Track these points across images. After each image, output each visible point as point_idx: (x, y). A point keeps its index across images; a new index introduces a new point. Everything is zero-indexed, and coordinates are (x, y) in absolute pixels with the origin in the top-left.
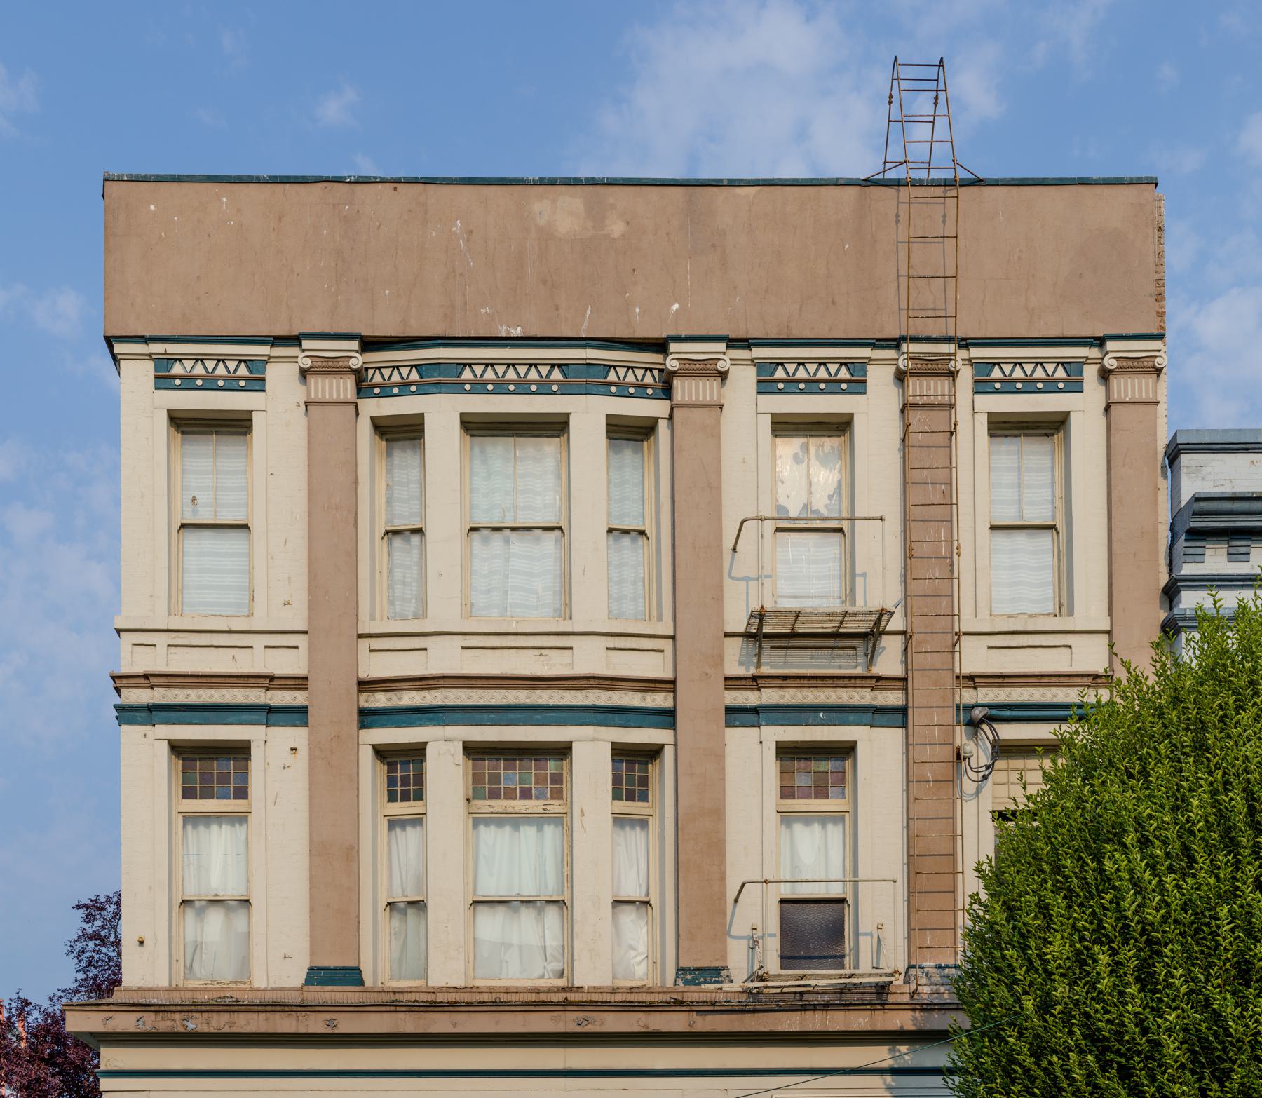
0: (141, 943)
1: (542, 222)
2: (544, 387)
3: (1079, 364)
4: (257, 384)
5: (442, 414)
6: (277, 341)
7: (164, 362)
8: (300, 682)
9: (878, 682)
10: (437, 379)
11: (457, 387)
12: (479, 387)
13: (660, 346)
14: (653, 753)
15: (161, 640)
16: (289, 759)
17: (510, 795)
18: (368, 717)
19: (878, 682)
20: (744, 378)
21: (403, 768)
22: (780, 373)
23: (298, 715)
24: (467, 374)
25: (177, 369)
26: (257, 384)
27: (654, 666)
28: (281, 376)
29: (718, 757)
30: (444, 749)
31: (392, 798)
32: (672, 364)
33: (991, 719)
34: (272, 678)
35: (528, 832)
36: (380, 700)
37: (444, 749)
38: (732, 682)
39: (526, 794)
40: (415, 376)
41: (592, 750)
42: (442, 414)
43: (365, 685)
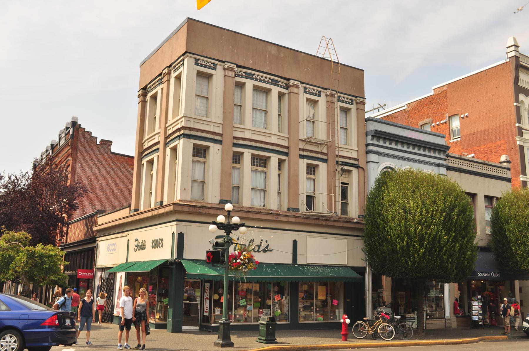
0: (185, 189)
1: (269, 50)
2: (268, 83)
3: (352, 100)
4: (215, 69)
5: (249, 84)
6: (220, 61)
7: (197, 60)
8: (221, 135)
9: (323, 154)
10: (249, 76)
11: (253, 79)
12: (256, 80)
13: (288, 80)
14: (284, 160)
15: (193, 120)
16: (217, 151)
17: (257, 166)
18: (235, 145)
19: (323, 154)
20: (301, 90)
21: (237, 158)
22: (307, 90)
23: (220, 142)
24: (254, 77)
25: (199, 62)
26: (215, 69)
27: (285, 144)
28: (219, 68)
29: (297, 164)
30: (248, 155)
31: (233, 163)
32: (291, 84)
33: (342, 165)
34: (216, 133)
35: (258, 174)
36: (235, 141)
37: (248, 155)
38: (300, 149)
39: (260, 166)
40: (244, 74)
41: (274, 159)
42: (249, 84)
43: (234, 138)
